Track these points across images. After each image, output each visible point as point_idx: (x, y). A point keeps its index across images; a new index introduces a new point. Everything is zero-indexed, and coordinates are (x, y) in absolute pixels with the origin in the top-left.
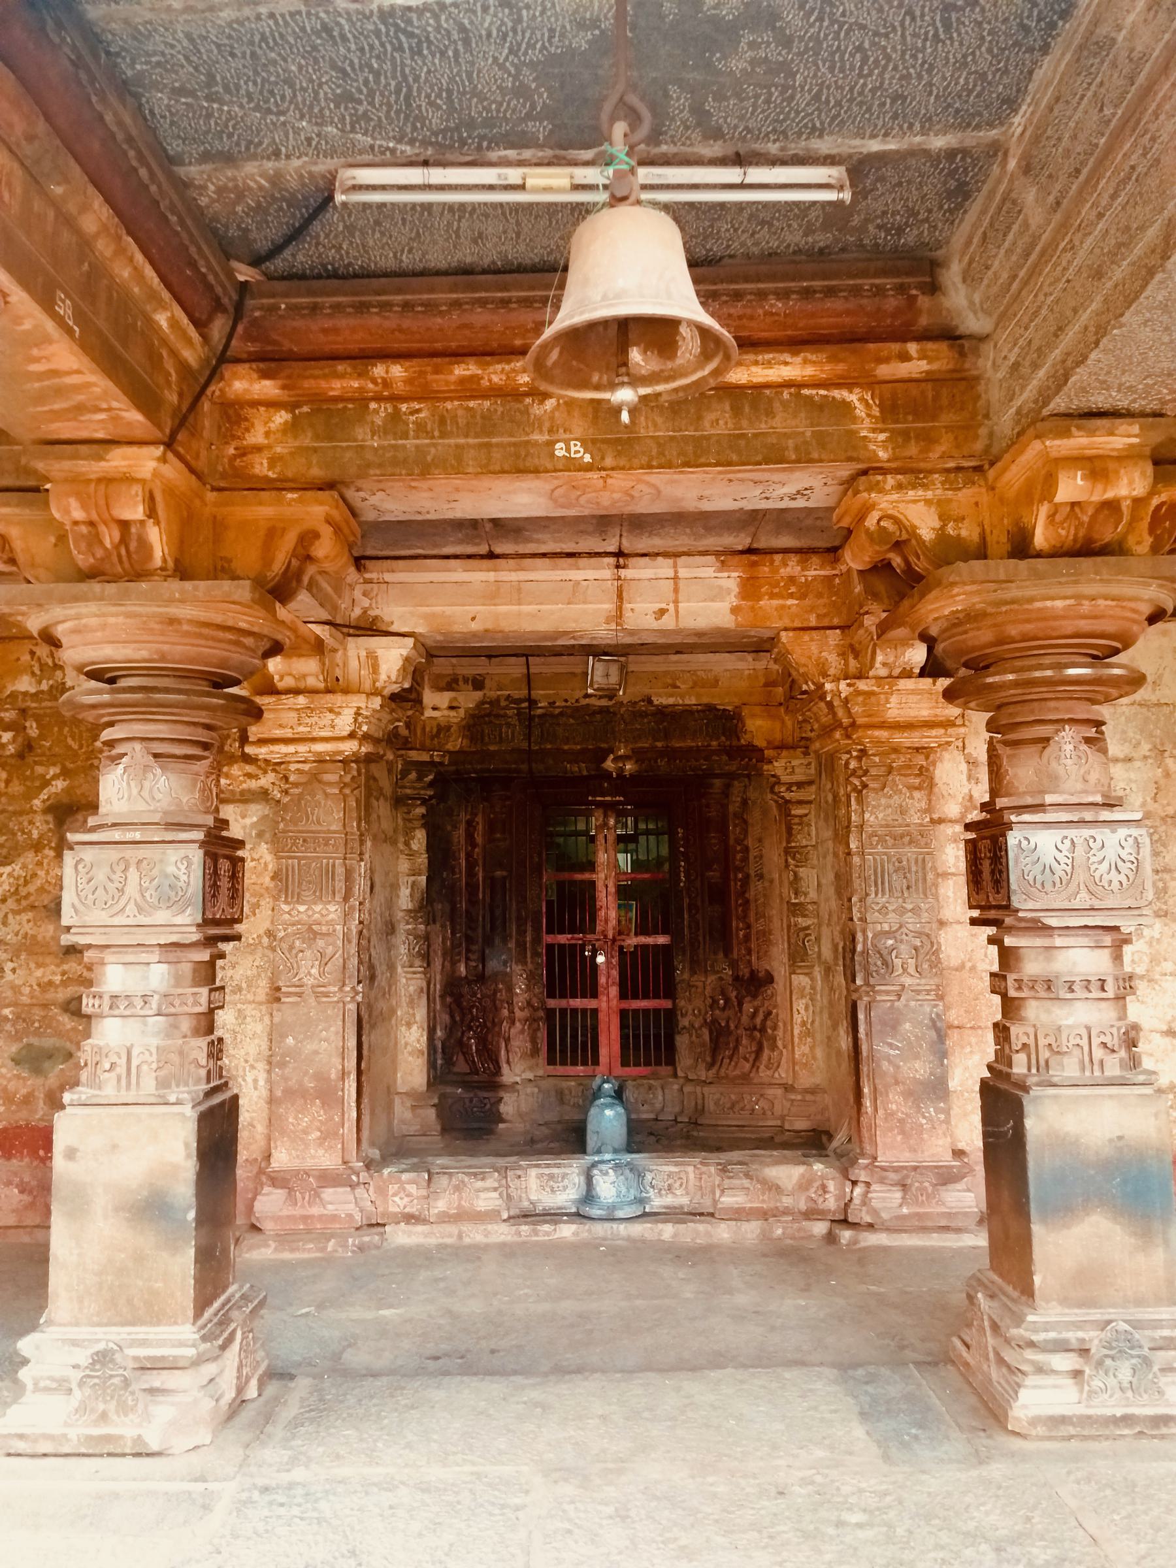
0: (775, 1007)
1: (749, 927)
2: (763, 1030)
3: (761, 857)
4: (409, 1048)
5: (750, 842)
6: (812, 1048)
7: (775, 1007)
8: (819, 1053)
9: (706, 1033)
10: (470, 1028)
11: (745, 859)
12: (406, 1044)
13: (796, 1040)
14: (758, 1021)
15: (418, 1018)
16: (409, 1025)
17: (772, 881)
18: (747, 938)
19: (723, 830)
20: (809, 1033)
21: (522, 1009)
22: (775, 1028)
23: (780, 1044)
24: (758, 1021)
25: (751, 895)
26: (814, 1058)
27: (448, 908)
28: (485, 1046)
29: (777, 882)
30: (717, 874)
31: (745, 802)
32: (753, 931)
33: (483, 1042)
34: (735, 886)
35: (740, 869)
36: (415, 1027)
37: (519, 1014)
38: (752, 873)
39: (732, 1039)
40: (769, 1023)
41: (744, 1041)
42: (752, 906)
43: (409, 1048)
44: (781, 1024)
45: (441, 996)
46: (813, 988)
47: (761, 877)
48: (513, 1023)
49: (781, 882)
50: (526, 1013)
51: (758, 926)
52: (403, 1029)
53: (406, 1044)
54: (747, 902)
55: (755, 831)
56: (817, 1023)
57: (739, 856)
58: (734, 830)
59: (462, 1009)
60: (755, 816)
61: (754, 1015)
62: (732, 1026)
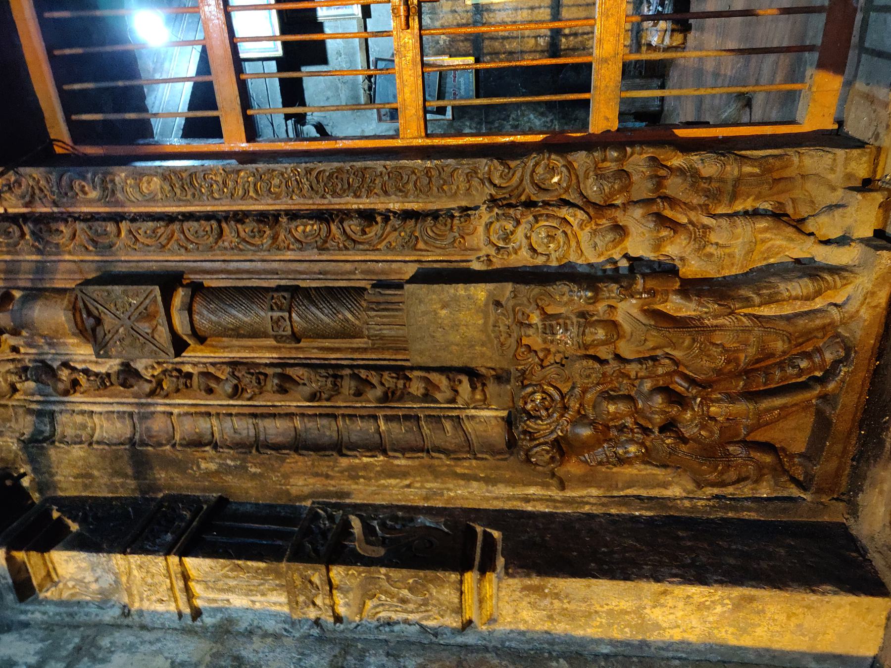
15: (625, 604)
27: (296, 461)
37: (639, 244)
48: (666, 270)
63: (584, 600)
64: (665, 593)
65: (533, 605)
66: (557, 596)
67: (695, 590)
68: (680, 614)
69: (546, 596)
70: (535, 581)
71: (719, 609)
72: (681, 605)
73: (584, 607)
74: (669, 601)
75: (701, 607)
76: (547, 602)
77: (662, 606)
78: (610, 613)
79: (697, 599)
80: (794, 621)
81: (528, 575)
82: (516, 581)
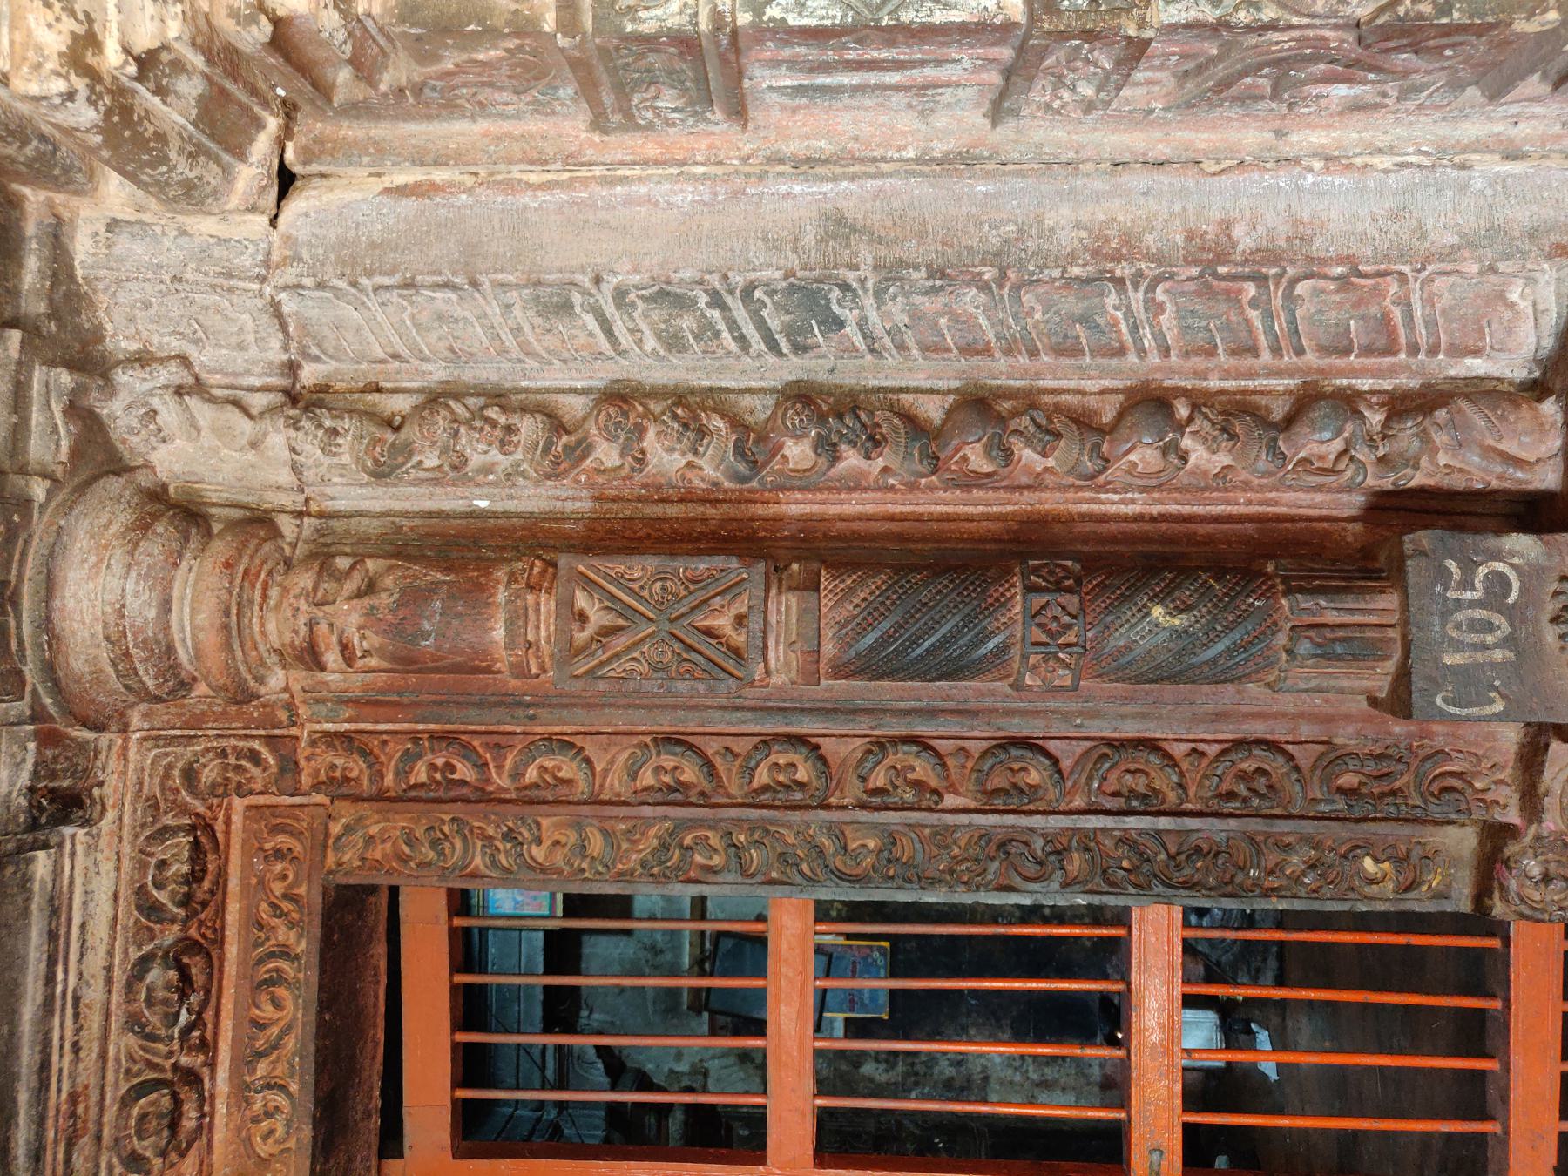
1: (1151, 403)
3: (668, 297)
5: (568, 370)
11: (690, 409)
17: (838, 226)
18: (1235, 414)
19: (460, 553)
25: (927, 380)
29: (846, 194)
30: (785, 608)
31: (301, 401)
32: (1177, 374)
34: (872, 488)
35: (754, 444)
38: (792, 368)
42: (1002, 372)
47: (811, 303)
49: (845, 162)
51: (1156, 338)
54: (978, 405)
55: (489, 338)
57: (666, 458)
58: (504, 482)
60: (367, 336)
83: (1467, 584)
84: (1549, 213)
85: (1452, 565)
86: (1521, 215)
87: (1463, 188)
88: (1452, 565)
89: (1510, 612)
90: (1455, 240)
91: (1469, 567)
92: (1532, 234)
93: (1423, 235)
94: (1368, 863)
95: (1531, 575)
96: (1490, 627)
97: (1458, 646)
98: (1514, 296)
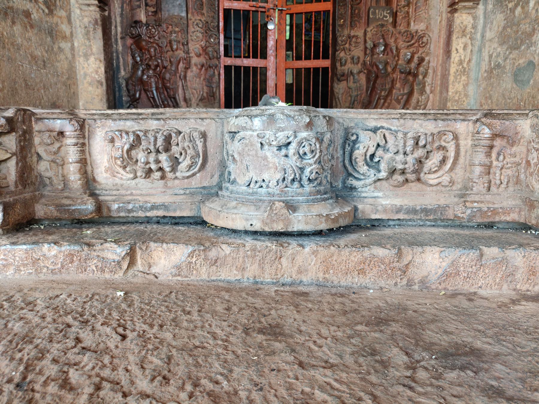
0: (428, 54)
2: (415, 76)
4: (88, 79)
6: (466, 86)
7: (428, 54)
8: (471, 89)
9: (363, 78)
10: (148, 66)
12: (86, 75)
13: (451, 78)
14: (413, 65)
15: (94, 50)
16: (86, 56)
20: (464, 72)
21: (199, 56)
22: (425, 75)
23: (428, 89)
24: (413, 65)
26: (466, 96)
28: (164, 84)
33: (161, 77)
36: (92, 59)
39: (389, 80)
40: (421, 69)
41: (398, 85)
43: (88, 79)
44: (430, 71)
45: (122, 38)
46: (474, 27)
50: (202, 60)
52: (81, 59)
53: (86, 75)
56: (473, 61)
59: (140, 48)
61: (409, 61)
62: (389, 69)
63: (94, 38)
64: (100, 61)
65: (90, 22)
66: (95, 29)
67: (103, 69)
68: (93, 66)
69: (94, 26)
70: (100, 22)
71: (97, 76)
72: (97, 66)
73: (92, 38)
74: (98, 62)
75: (97, 72)
76: (92, 26)
77: (96, 61)
78: (91, 46)
79: (99, 71)
80: (96, 97)
81: (101, 21)
82: (99, 17)
83: (386, 13)
84: (432, 26)
85: (389, 11)
86: (432, 22)
87: (437, 15)
88: (389, 11)
89: (383, 18)
90: (430, 13)
91: (388, 13)
92: (430, 24)
93: (431, 9)
94: (342, 21)
95: (387, 21)
96: (381, 15)
97: (379, 12)
98: (422, 24)
